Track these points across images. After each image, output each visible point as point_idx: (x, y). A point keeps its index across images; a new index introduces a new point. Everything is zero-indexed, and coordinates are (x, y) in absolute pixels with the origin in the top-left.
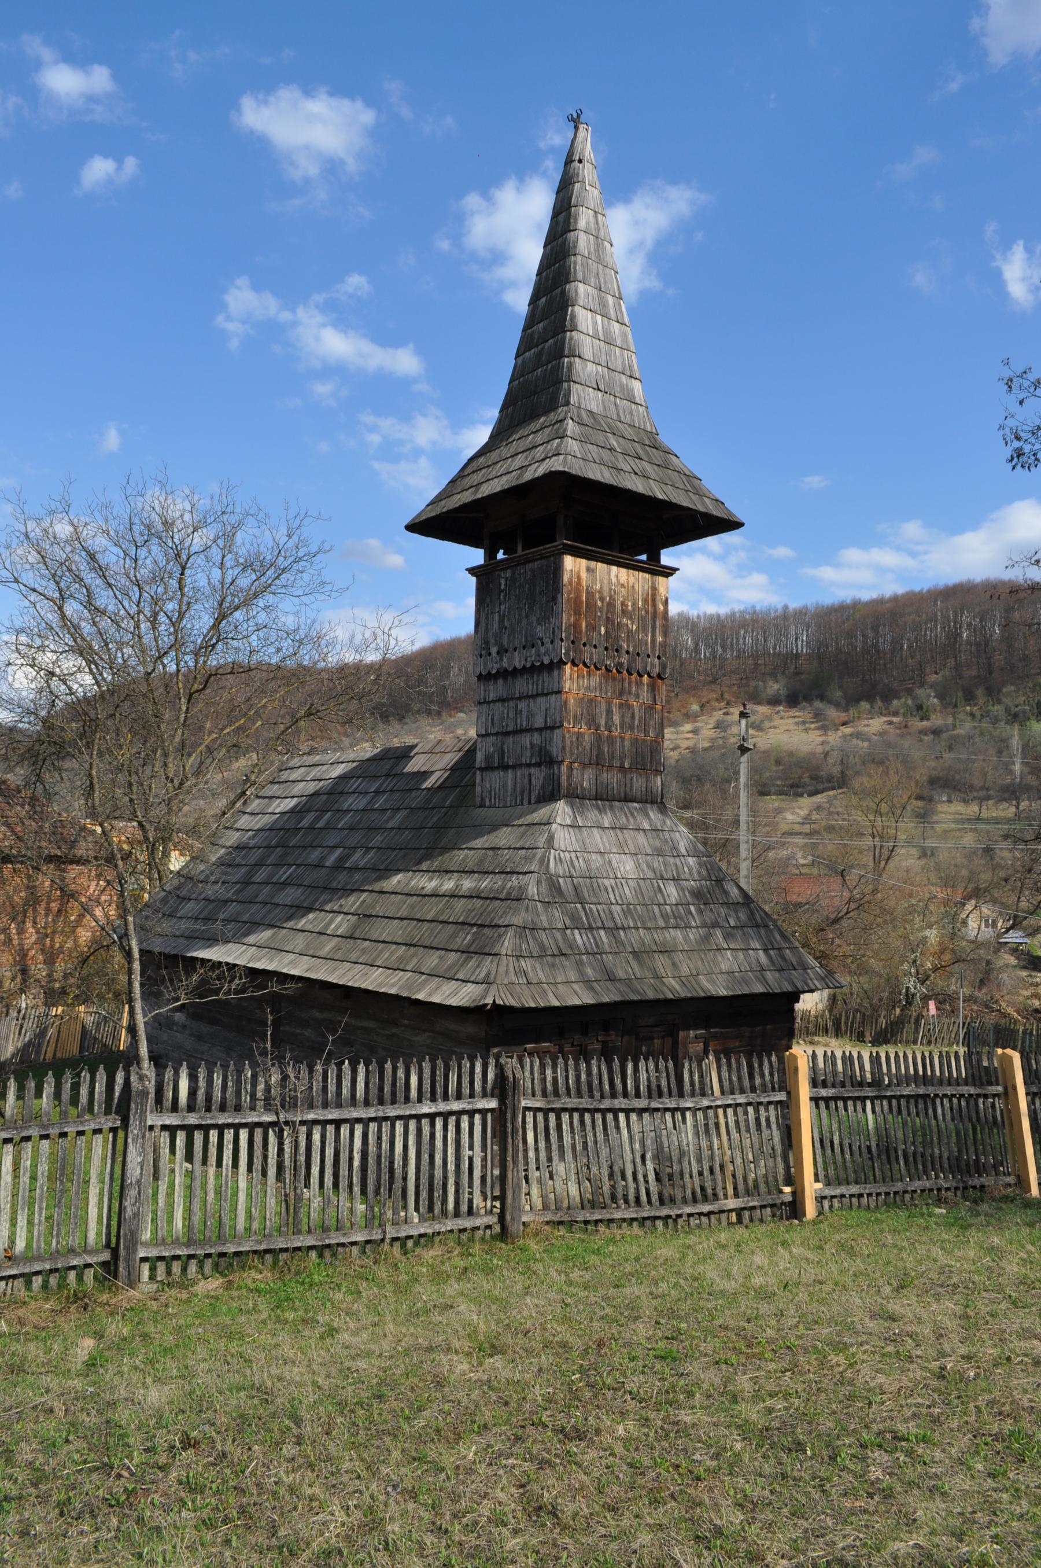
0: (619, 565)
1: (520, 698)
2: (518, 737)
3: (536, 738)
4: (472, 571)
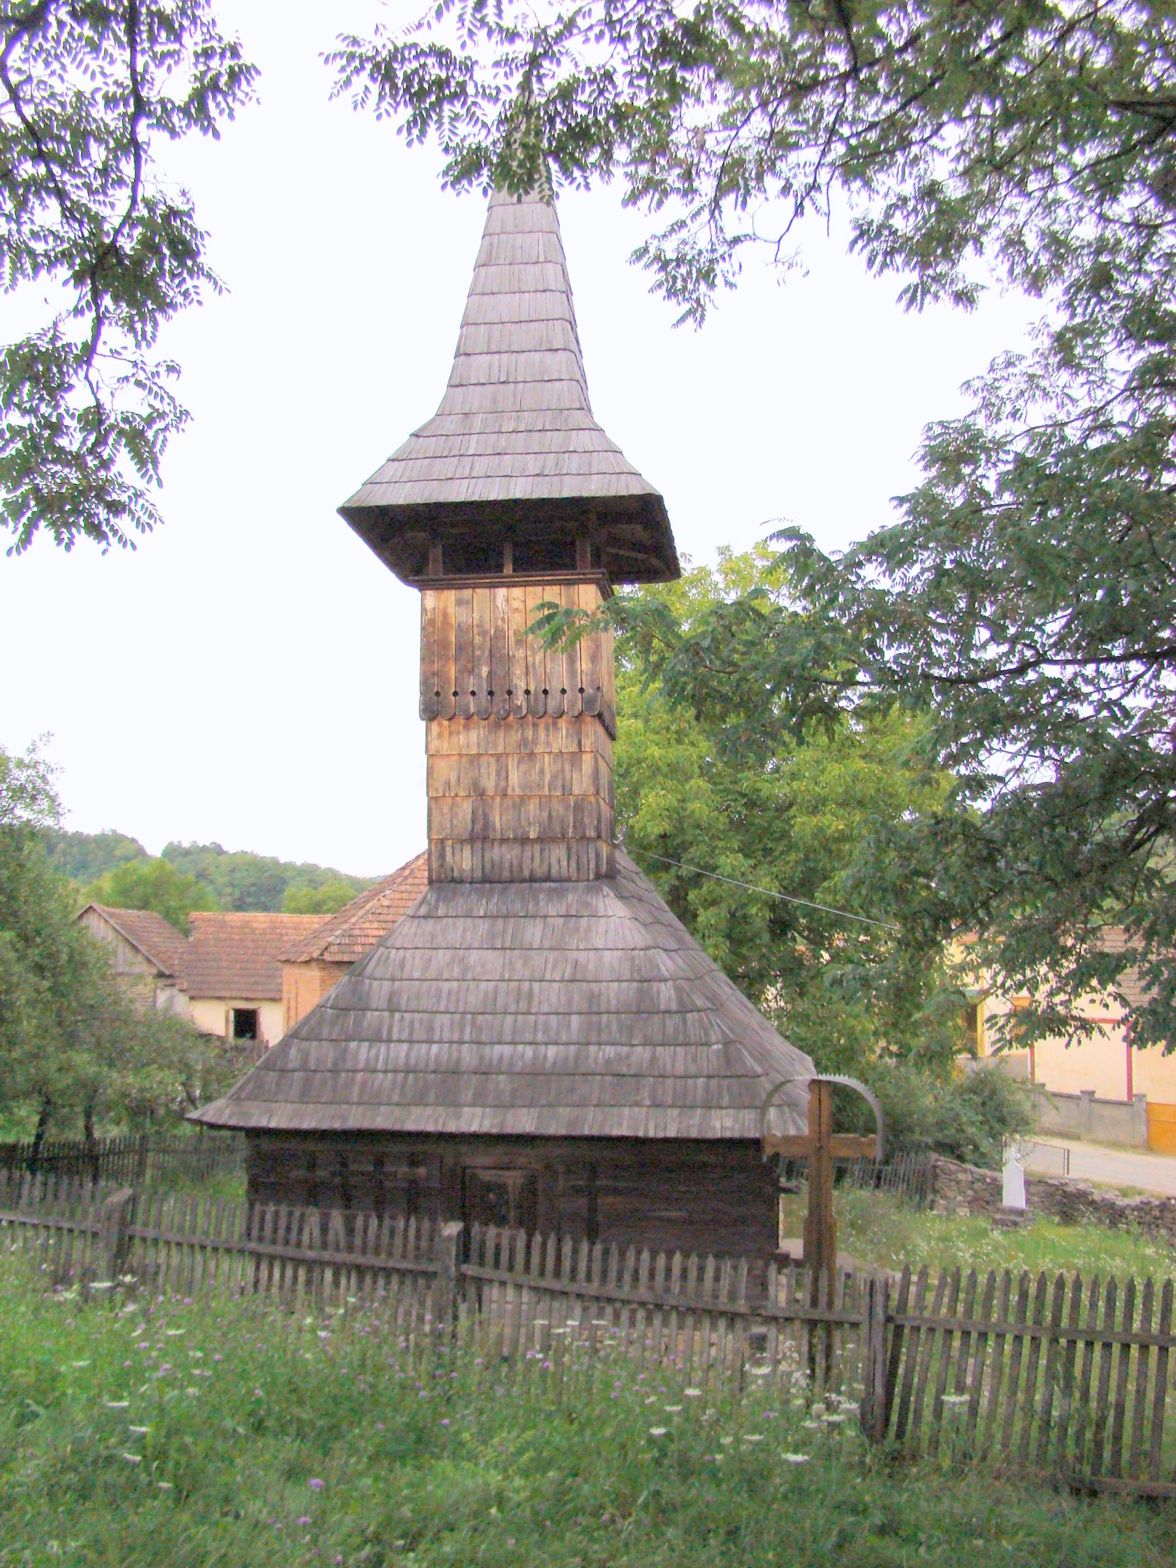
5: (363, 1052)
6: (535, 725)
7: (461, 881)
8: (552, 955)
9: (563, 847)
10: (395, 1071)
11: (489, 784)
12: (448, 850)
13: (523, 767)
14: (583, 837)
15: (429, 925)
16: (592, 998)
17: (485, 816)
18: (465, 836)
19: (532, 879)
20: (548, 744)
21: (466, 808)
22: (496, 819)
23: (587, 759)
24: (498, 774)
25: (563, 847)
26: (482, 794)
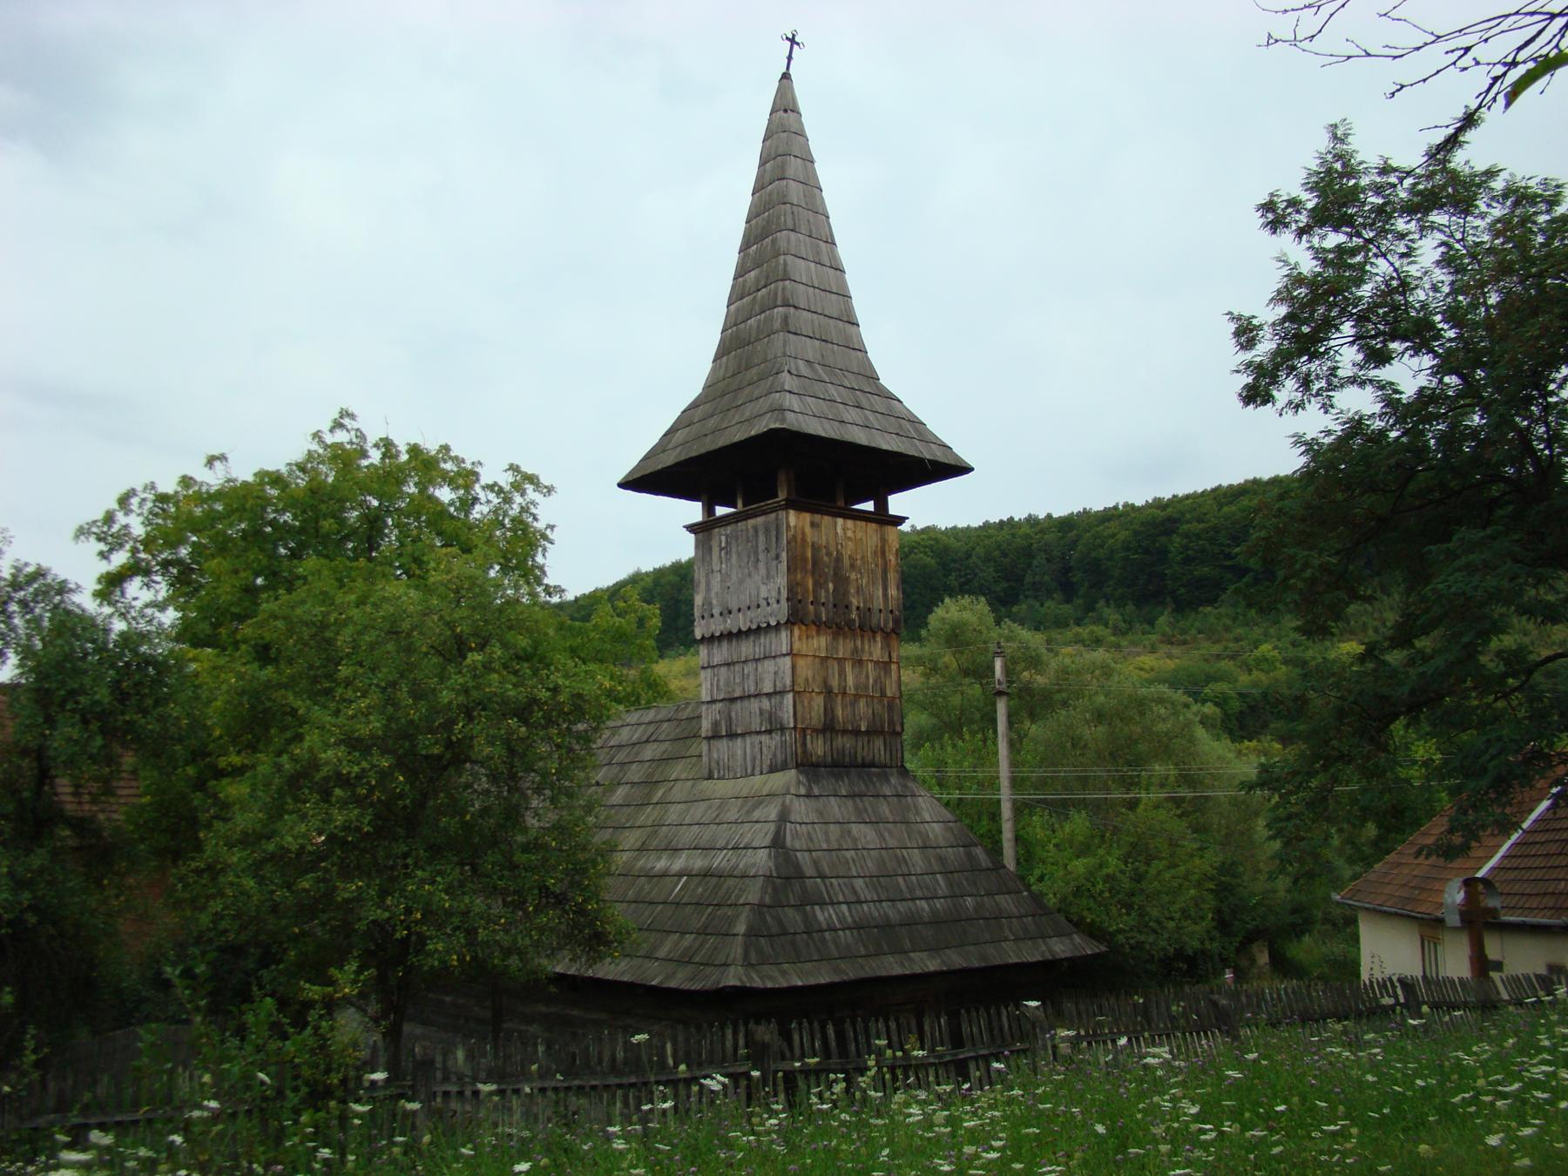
1: (744, 662)
2: (746, 703)
3: (766, 704)
4: (692, 528)
5: (821, 915)
7: (817, 765)
8: (903, 827)
10: (850, 928)
11: (835, 683)
15: (811, 803)
16: (941, 860)
19: (864, 765)
21: (819, 701)
22: (839, 712)
23: (894, 667)
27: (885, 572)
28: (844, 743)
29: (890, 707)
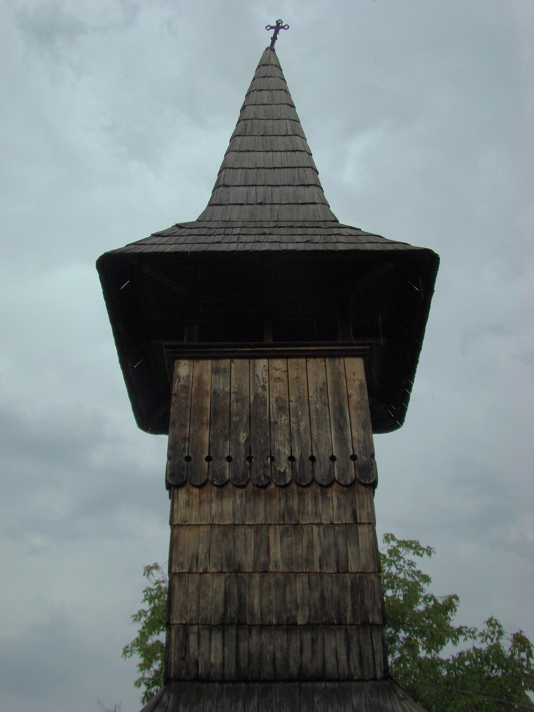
0: (269, 356)
6: (301, 495)
7: (208, 680)
9: (340, 635)
11: (247, 559)
12: (193, 638)
13: (287, 540)
14: (366, 624)
17: (241, 596)
18: (215, 620)
19: (302, 677)
20: (316, 514)
21: (217, 586)
24: (257, 547)
25: (340, 635)
26: (237, 570)
27: (340, 410)
28: (269, 646)
29: (357, 588)
